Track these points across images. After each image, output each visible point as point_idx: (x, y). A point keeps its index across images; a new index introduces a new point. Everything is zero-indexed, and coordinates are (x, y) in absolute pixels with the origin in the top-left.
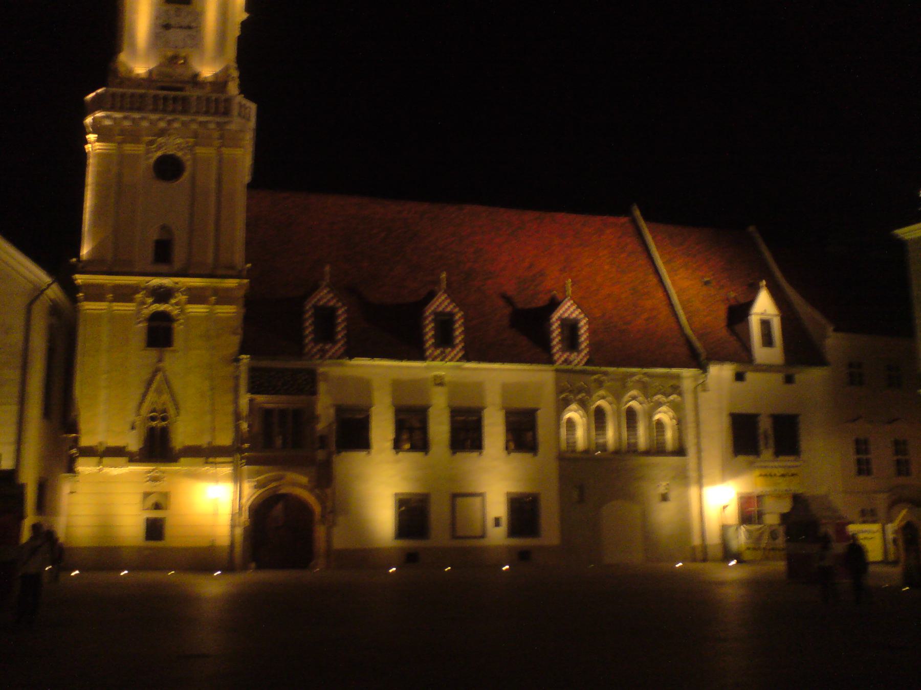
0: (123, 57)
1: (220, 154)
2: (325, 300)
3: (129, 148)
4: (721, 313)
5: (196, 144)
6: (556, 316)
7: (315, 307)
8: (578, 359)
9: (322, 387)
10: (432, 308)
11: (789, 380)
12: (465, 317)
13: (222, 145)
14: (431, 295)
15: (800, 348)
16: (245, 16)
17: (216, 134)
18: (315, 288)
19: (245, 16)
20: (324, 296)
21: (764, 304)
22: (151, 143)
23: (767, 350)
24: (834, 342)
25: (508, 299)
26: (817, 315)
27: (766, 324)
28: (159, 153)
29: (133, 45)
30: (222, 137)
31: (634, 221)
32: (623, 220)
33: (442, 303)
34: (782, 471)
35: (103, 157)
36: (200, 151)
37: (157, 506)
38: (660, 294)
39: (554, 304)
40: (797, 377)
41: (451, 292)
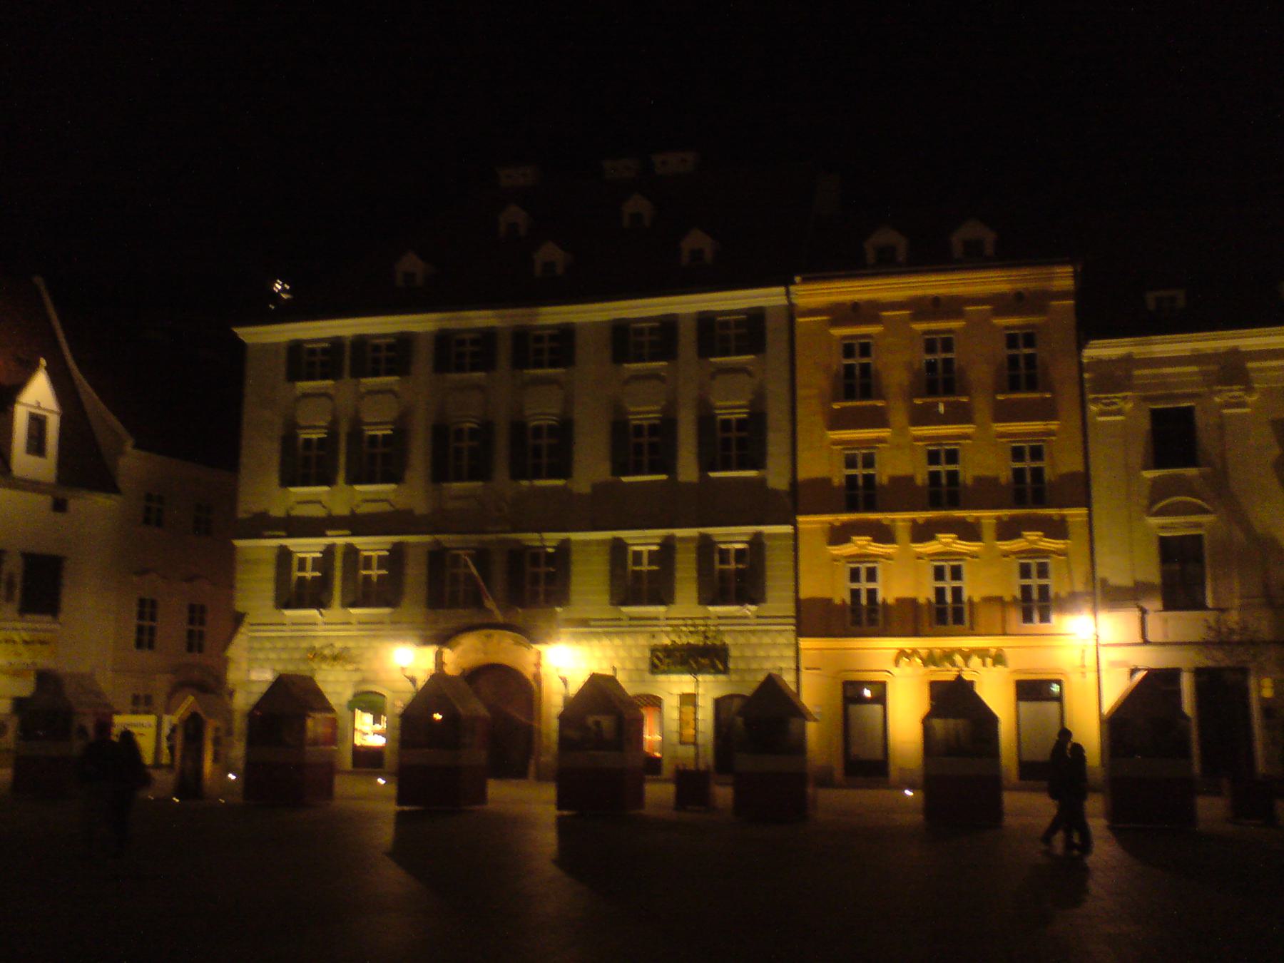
11: (60, 506)
15: (83, 463)
21: (38, 392)
23: (34, 460)
24: (132, 462)
26: (113, 420)
27: (37, 423)
34: (26, 636)
40: (73, 504)
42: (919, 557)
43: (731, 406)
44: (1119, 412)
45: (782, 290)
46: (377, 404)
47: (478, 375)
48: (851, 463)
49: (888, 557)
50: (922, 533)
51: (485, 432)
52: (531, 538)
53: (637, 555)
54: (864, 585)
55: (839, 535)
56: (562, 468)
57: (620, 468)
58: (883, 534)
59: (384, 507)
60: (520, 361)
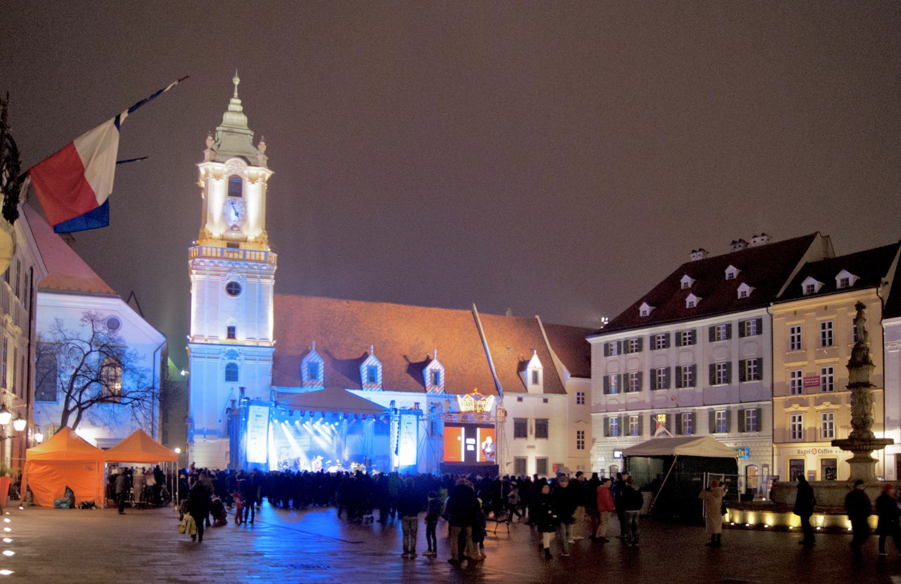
0: (207, 226)
1: (260, 282)
4: (515, 365)
7: (308, 362)
12: (382, 368)
14: (365, 356)
18: (307, 352)
25: (405, 357)
29: (212, 220)
31: (473, 313)
32: (469, 312)
33: (371, 361)
35: (202, 283)
38: (484, 355)
39: (428, 361)
41: (376, 354)
42: (817, 411)
43: (750, 355)
44: (897, 349)
45: (765, 309)
46: (633, 363)
47: (665, 350)
48: (793, 375)
49: (806, 412)
50: (818, 402)
51: (667, 370)
52: (682, 410)
53: (719, 414)
54: (797, 423)
55: (788, 404)
56: (693, 384)
57: (712, 382)
58: (804, 403)
59: (636, 400)
60: (678, 343)
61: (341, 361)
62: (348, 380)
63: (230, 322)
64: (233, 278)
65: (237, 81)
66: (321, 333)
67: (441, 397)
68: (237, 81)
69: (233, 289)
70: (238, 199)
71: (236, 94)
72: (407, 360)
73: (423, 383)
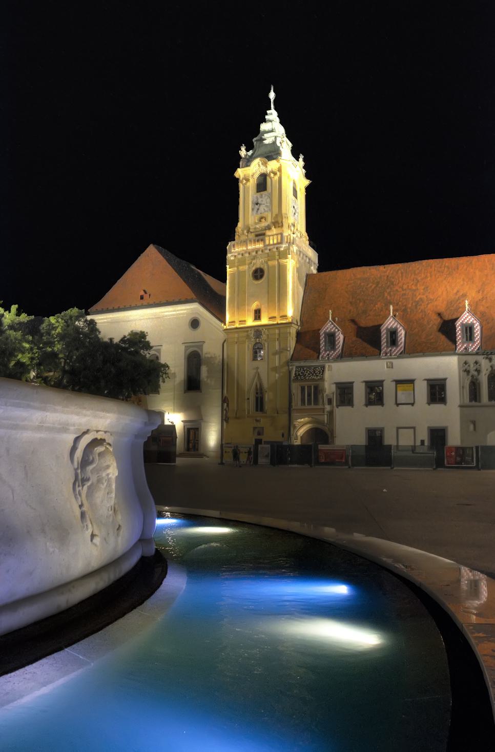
2: (329, 329)
3: (241, 268)
5: (269, 260)
6: (458, 323)
8: (474, 347)
9: (327, 374)
10: (385, 327)
13: (280, 258)
16: (307, 182)
17: (277, 253)
19: (307, 182)
20: (329, 327)
22: (251, 263)
25: (439, 314)
28: (254, 268)
30: (279, 255)
35: (233, 275)
36: (270, 263)
37: (259, 434)
61: (365, 328)
62: (369, 346)
63: (255, 306)
64: (258, 263)
65: (272, 95)
66: (351, 303)
67: (477, 354)
68: (272, 95)
69: (259, 274)
70: (264, 193)
71: (272, 106)
72: (441, 317)
73: (454, 341)
